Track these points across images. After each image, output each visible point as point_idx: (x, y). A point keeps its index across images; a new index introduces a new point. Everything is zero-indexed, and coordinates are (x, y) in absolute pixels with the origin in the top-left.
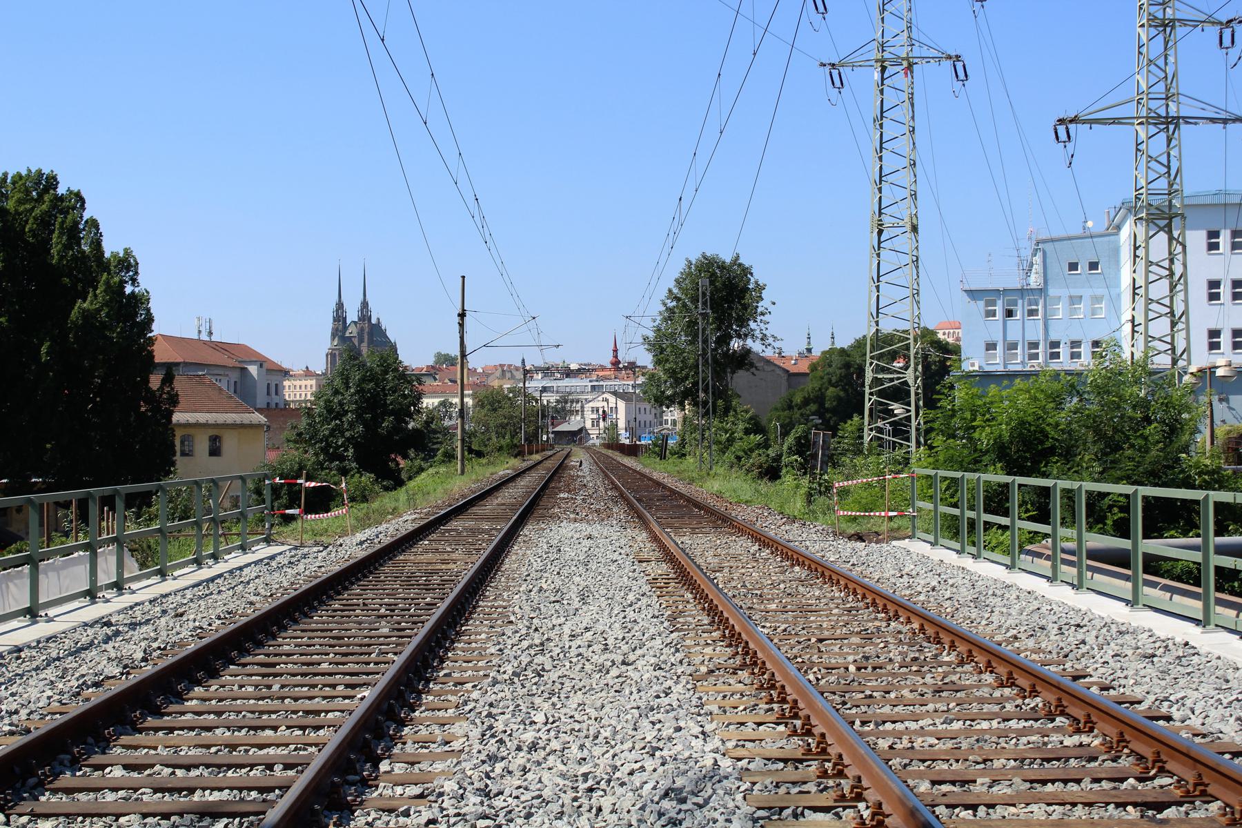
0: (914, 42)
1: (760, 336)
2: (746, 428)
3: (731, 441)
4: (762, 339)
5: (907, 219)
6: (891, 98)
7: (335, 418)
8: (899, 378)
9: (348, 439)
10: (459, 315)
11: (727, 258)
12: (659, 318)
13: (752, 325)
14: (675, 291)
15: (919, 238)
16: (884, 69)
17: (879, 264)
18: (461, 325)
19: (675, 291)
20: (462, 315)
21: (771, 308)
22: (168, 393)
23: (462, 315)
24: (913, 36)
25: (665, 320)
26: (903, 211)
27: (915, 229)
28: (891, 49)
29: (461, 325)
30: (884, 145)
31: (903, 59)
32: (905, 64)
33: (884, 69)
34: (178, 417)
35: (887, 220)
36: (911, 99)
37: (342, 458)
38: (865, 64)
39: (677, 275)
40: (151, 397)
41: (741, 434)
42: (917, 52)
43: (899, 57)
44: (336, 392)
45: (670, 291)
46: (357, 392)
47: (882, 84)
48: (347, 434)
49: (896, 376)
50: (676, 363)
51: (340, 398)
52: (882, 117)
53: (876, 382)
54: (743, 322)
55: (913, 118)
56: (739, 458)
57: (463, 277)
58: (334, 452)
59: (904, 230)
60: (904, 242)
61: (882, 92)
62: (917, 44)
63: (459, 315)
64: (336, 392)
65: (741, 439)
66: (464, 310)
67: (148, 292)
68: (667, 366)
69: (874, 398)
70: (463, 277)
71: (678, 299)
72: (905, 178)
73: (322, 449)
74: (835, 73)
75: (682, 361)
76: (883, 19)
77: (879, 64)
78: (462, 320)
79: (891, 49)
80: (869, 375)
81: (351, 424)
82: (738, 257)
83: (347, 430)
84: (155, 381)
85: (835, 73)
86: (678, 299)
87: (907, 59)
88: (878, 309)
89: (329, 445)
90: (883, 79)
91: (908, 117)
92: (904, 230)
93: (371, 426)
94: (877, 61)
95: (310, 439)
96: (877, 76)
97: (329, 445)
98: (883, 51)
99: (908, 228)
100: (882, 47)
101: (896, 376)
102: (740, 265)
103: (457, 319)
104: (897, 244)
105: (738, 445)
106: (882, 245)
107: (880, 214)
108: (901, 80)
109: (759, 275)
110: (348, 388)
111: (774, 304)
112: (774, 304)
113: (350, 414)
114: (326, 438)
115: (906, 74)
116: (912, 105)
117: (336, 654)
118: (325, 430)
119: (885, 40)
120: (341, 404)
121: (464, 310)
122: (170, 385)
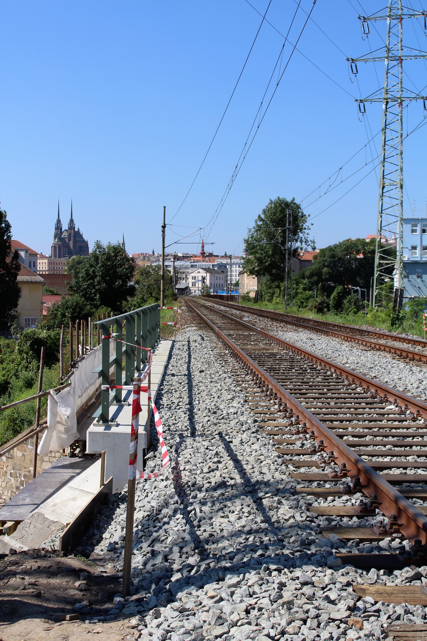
0: (403, 89)
1: (304, 240)
2: (304, 288)
3: (297, 294)
4: (305, 242)
5: (398, 181)
6: (390, 117)
7: (90, 279)
8: (392, 263)
9: (97, 290)
10: (162, 227)
11: (289, 200)
12: (253, 230)
13: (301, 235)
14: (263, 216)
15: (403, 191)
16: (387, 103)
17: (382, 204)
18: (163, 232)
19: (263, 216)
20: (164, 227)
21: (311, 227)
22: (15, 264)
23: (164, 227)
24: (403, 86)
25: (257, 231)
26: (396, 177)
27: (402, 187)
28: (392, 93)
29: (163, 232)
30: (386, 143)
31: (398, 98)
32: (399, 101)
33: (387, 103)
34: (20, 278)
35: (387, 182)
36: (401, 119)
37: (93, 299)
38: (379, 101)
39: (265, 208)
40: (5, 266)
41: (301, 291)
42: (405, 94)
43: (396, 97)
44: (91, 266)
45: (259, 216)
46: (102, 266)
47: (386, 111)
48: (97, 287)
49: (390, 262)
50: (262, 254)
51: (93, 269)
52: (386, 128)
53: (380, 265)
54: (295, 233)
55: (402, 130)
56: (302, 303)
57: (165, 207)
58: (89, 296)
59: (396, 186)
60: (396, 193)
61: (386, 115)
62: (405, 90)
63: (162, 227)
64: (91, 266)
65: (302, 293)
66: (165, 224)
67: (5, 212)
68: (257, 255)
69: (378, 272)
70: (165, 207)
71: (262, 220)
72: (396, 160)
73: (83, 295)
74: (362, 105)
75: (265, 253)
76: (387, 77)
77: (386, 101)
78: (164, 229)
79: (392, 93)
80: (377, 261)
81: (99, 282)
82: (294, 199)
83: (97, 285)
84: (8, 260)
85: (362, 105)
86: (263, 220)
87: (400, 98)
88: (381, 227)
89: (86, 293)
90: (386, 108)
91: (400, 129)
92: (396, 186)
93: (110, 284)
94: (385, 99)
95: (77, 290)
96: (384, 107)
97: (86, 293)
98: (387, 94)
99: (399, 186)
100: (387, 92)
101: (390, 262)
102: (295, 203)
103: (161, 229)
104: (391, 194)
105: (300, 296)
106: (384, 194)
107: (383, 178)
108: (396, 109)
109: (305, 210)
110: (98, 263)
111: (312, 224)
112: (312, 224)
113: (98, 278)
114: (85, 289)
115: (399, 106)
116: (402, 122)
117: (355, 403)
118: (85, 285)
119: (388, 88)
120: (94, 272)
121: (165, 224)
122: (16, 261)
